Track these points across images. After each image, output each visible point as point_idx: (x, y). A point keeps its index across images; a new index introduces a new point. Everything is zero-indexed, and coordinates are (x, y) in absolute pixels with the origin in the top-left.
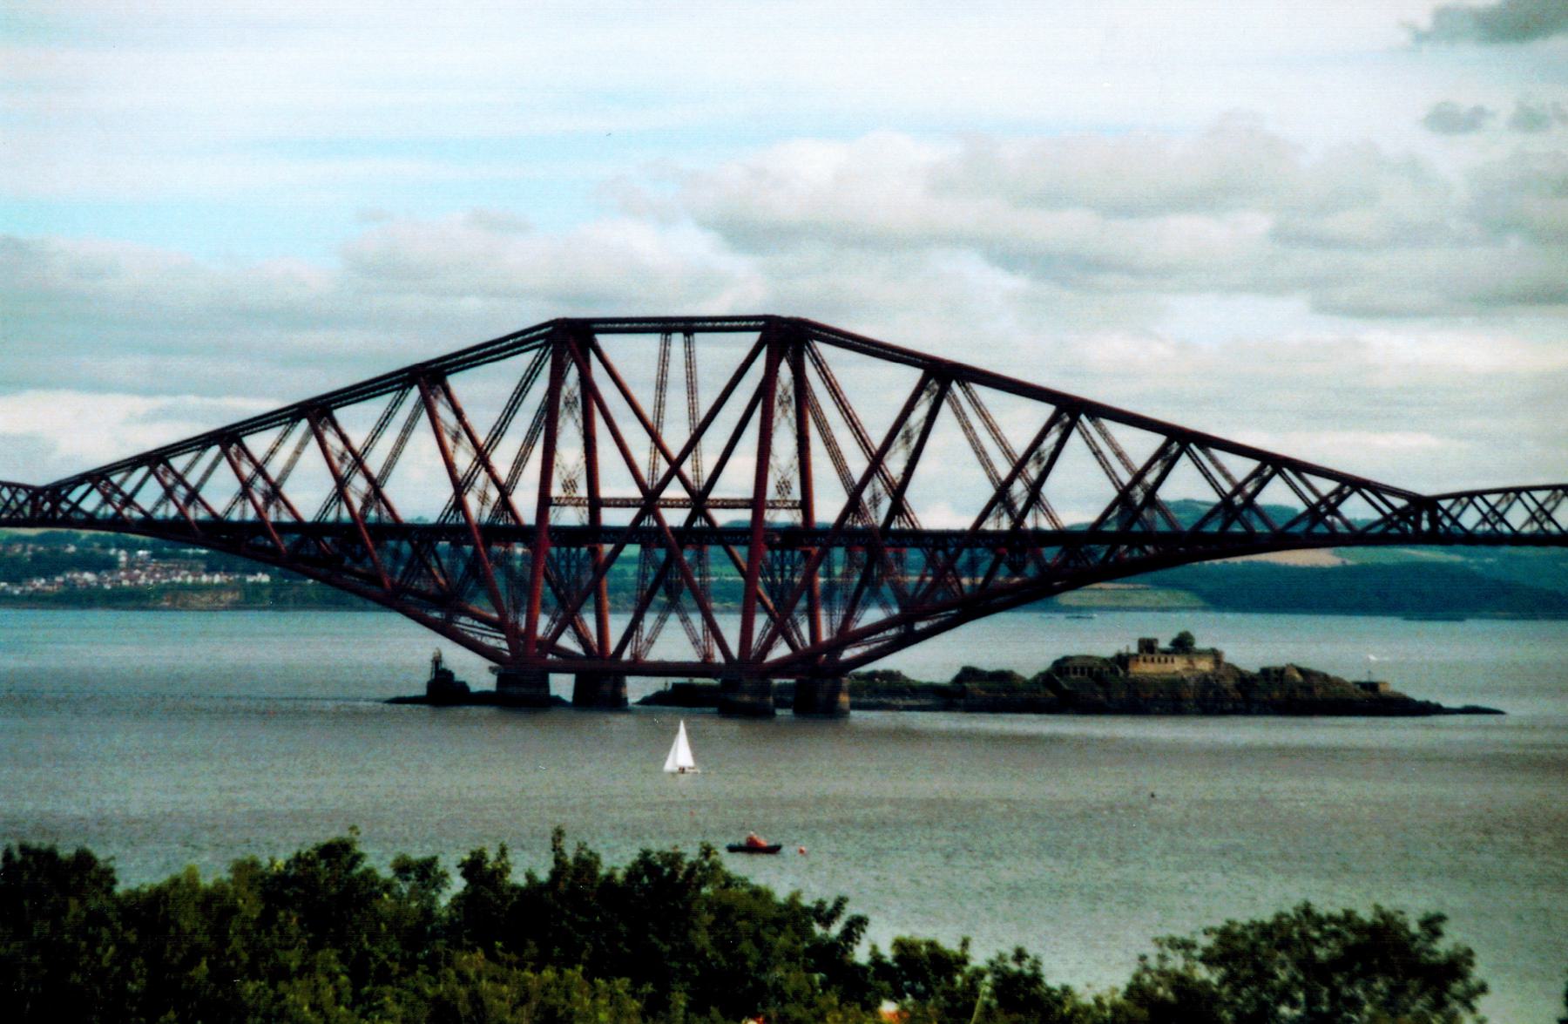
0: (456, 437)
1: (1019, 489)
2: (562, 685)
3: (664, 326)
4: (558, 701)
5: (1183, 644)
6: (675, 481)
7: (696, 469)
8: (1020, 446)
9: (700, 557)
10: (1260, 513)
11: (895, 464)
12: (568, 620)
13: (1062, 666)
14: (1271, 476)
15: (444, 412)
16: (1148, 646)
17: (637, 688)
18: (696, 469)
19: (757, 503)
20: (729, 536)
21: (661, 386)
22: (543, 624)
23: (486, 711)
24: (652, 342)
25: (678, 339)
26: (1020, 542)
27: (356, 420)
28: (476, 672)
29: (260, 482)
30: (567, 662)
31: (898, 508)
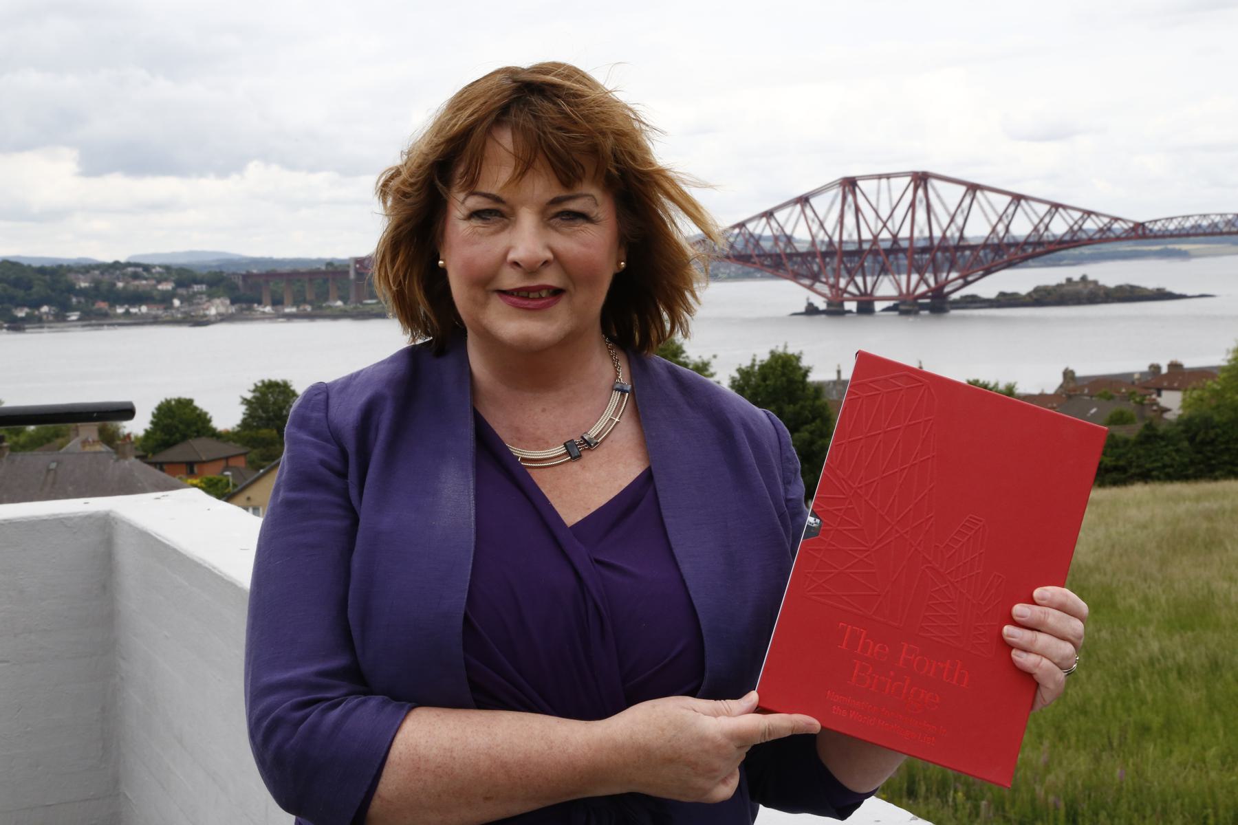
0: (813, 221)
1: (1001, 229)
2: (851, 306)
3: (880, 177)
4: (850, 312)
5: (1084, 278)
6: (885, 230)
7: (893, 226)
8: (1001, 211)
9: (897, 259)
10: (1084, 231)
11: (959, 220)
12: (852, 280)
13: (1037, 290)
14: (1086, 219)
15: (808, 211)
16: (1069, 280)
17: (879, 306)
18: (893, 226)
19: (911, 238)
20: (904, 250)
21: (878, 200)
22: (842, 283)
23: (823, 316)
24: (875, 182)
25: (884, 181)
26: (1040, 243)
27: (780, 216)
28: (821, 304)
29: (752, 240)
30: (853, 297)
31: (962, 237)
